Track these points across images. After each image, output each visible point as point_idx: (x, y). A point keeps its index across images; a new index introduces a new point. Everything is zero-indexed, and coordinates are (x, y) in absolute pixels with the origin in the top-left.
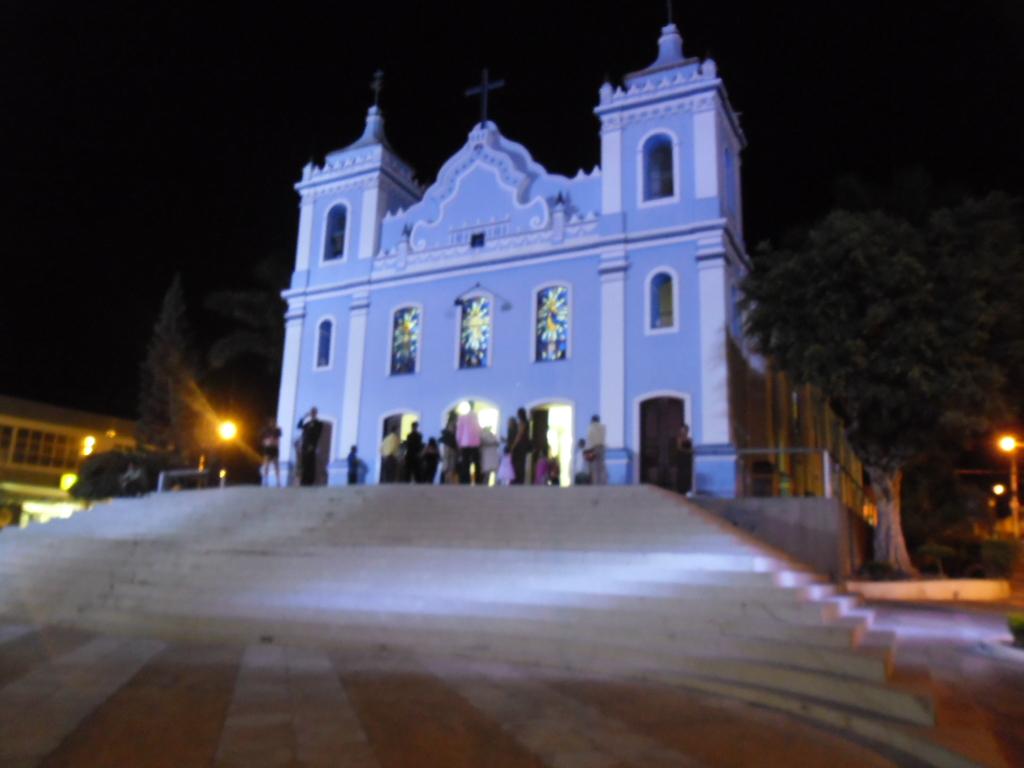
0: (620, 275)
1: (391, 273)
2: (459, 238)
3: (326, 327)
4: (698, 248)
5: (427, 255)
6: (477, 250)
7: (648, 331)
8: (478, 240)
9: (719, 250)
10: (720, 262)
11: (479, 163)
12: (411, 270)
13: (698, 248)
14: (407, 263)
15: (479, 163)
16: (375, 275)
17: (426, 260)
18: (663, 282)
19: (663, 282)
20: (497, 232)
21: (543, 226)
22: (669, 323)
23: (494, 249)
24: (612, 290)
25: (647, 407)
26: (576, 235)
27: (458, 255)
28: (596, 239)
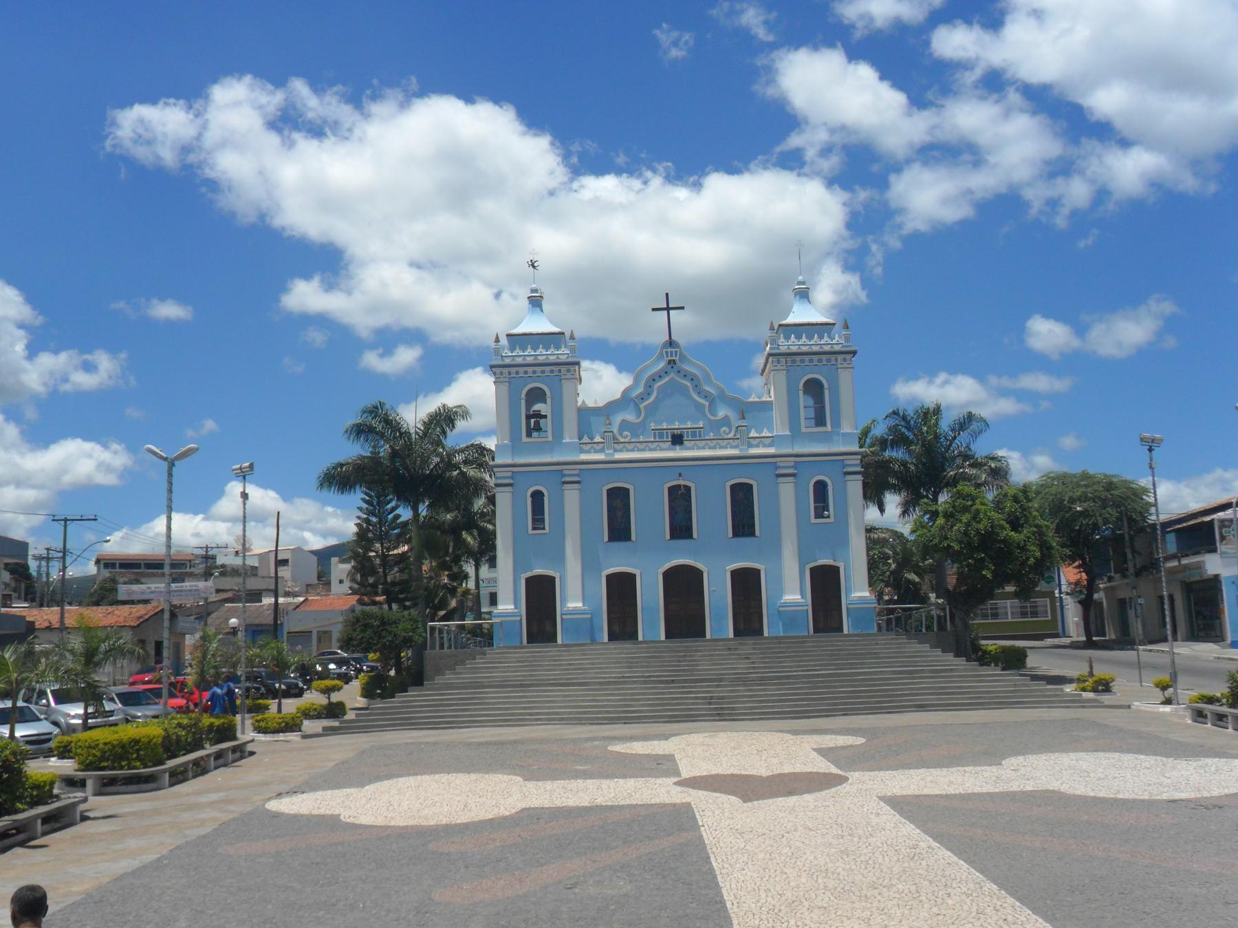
0: (791, 479)
1: (601, 457)
2: (661, 436)
3: (537, 497)
4: (845, 466)
5: (630, 446)
6: (678, 447)
7: (813, 520)
8: (677, 440)
9: (859, 469)
10: (860, 477)
11: (672, 375)
12: (618, 456)
13: (845, 466)
14: (616, 451)
15: (672, 375)
16: (584, 457)
17: (633, 450)
18: (821, 488)
19: (821, 488)
20: (694, 434)
21: (731, 436)
22: (828, 517)
23: (692, 448)
24: (787, 490)
25: (814, 571)
26: (757, 446)
27: (661, 449)
28: (772, 451)
